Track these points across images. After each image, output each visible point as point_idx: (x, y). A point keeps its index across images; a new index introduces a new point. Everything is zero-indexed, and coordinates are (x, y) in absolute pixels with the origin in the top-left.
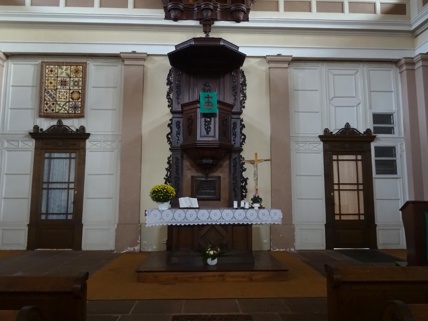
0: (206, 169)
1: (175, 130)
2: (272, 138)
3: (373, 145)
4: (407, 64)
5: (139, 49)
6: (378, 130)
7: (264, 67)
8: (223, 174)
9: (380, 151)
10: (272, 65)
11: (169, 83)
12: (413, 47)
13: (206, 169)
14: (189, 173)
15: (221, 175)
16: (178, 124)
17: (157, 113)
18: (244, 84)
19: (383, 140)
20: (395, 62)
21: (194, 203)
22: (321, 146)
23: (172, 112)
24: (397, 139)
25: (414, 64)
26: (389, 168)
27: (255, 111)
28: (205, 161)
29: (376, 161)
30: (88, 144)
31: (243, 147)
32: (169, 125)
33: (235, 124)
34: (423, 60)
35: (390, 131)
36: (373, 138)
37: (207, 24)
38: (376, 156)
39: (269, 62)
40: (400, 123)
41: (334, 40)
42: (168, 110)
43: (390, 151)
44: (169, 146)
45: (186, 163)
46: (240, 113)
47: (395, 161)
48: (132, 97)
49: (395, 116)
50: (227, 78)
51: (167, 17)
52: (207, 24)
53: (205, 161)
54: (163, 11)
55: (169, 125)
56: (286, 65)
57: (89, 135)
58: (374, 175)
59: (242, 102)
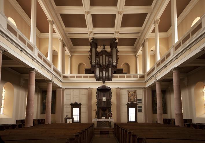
0: (104, 111)
1: (98, 103)
2: (117, 105)
3: (137, 106)
4: (144, 89)
5: (91, 87)
6: (138, 103)
7: (115, 90)
8: (107, 112)
9: (139, 107)
10: (117, 90)
11: (97, 94)
12: (146, 85)
13: (104, 111)
14: (101, 112)
15: (107, 112)
16: (99, 102)
17: (94, 100)
18: (111, 94)
19: (139, 105)
20: (142, 88)
21: (104, 118)
22: (127, 106)
23: (97, 100)
24: (142, 105)
25: (145, 89)
26: (140, 111)
27: (114, 99)
28: (104, 110)
29: (138, 109)
30: (81, 106)
31: (111, 107)
32: (97, 102)
33: (109, 102)
34: (147, 88)
35: (141, 103)
36: (137, 104)
37: (104, 82)
38: (138, 108)
39: (117, 89)
40: (143, 101)
41: (129, 84)
42: (97, 99)
43: (141, 107)
44: (97, 107)
45: (100, 110)
46: (110, 100)
47: (142, 109)
48: (90, 97)
49: (142, 100)
50: (108, 93)
51: (96, 81)
52: (104, 82)
53: (104, 110)
54: (95, 79)
55: (97, 102)
56: (119, 90)
57: (81, 104)
58: (137, 112)
59: (111, 97)
